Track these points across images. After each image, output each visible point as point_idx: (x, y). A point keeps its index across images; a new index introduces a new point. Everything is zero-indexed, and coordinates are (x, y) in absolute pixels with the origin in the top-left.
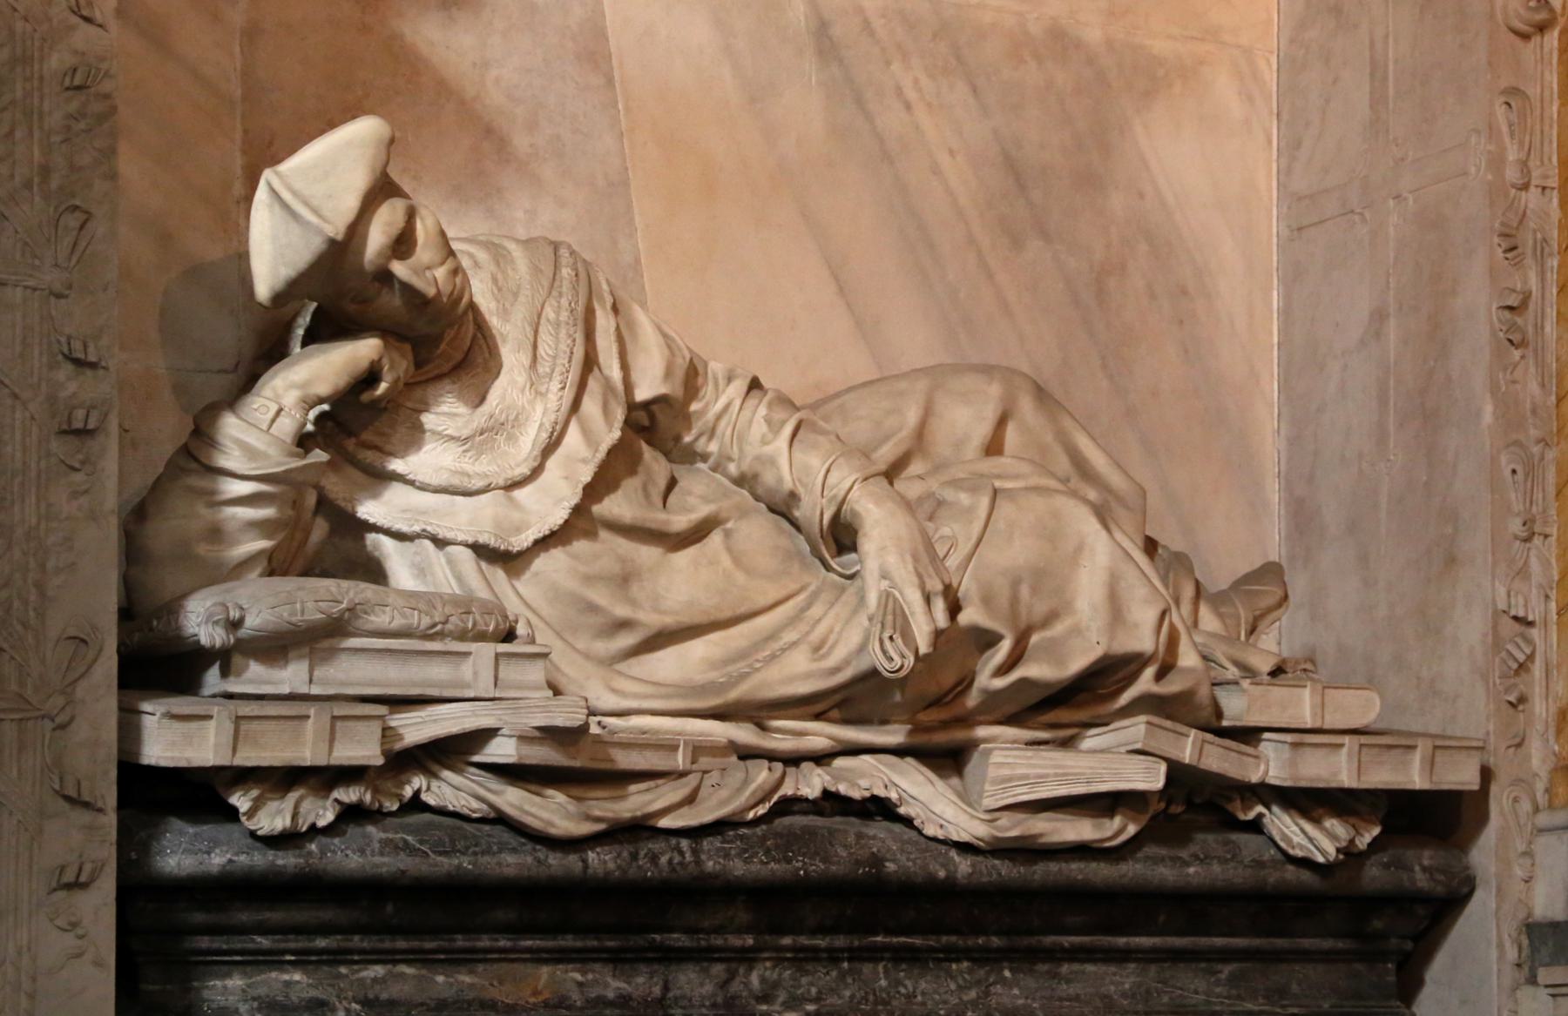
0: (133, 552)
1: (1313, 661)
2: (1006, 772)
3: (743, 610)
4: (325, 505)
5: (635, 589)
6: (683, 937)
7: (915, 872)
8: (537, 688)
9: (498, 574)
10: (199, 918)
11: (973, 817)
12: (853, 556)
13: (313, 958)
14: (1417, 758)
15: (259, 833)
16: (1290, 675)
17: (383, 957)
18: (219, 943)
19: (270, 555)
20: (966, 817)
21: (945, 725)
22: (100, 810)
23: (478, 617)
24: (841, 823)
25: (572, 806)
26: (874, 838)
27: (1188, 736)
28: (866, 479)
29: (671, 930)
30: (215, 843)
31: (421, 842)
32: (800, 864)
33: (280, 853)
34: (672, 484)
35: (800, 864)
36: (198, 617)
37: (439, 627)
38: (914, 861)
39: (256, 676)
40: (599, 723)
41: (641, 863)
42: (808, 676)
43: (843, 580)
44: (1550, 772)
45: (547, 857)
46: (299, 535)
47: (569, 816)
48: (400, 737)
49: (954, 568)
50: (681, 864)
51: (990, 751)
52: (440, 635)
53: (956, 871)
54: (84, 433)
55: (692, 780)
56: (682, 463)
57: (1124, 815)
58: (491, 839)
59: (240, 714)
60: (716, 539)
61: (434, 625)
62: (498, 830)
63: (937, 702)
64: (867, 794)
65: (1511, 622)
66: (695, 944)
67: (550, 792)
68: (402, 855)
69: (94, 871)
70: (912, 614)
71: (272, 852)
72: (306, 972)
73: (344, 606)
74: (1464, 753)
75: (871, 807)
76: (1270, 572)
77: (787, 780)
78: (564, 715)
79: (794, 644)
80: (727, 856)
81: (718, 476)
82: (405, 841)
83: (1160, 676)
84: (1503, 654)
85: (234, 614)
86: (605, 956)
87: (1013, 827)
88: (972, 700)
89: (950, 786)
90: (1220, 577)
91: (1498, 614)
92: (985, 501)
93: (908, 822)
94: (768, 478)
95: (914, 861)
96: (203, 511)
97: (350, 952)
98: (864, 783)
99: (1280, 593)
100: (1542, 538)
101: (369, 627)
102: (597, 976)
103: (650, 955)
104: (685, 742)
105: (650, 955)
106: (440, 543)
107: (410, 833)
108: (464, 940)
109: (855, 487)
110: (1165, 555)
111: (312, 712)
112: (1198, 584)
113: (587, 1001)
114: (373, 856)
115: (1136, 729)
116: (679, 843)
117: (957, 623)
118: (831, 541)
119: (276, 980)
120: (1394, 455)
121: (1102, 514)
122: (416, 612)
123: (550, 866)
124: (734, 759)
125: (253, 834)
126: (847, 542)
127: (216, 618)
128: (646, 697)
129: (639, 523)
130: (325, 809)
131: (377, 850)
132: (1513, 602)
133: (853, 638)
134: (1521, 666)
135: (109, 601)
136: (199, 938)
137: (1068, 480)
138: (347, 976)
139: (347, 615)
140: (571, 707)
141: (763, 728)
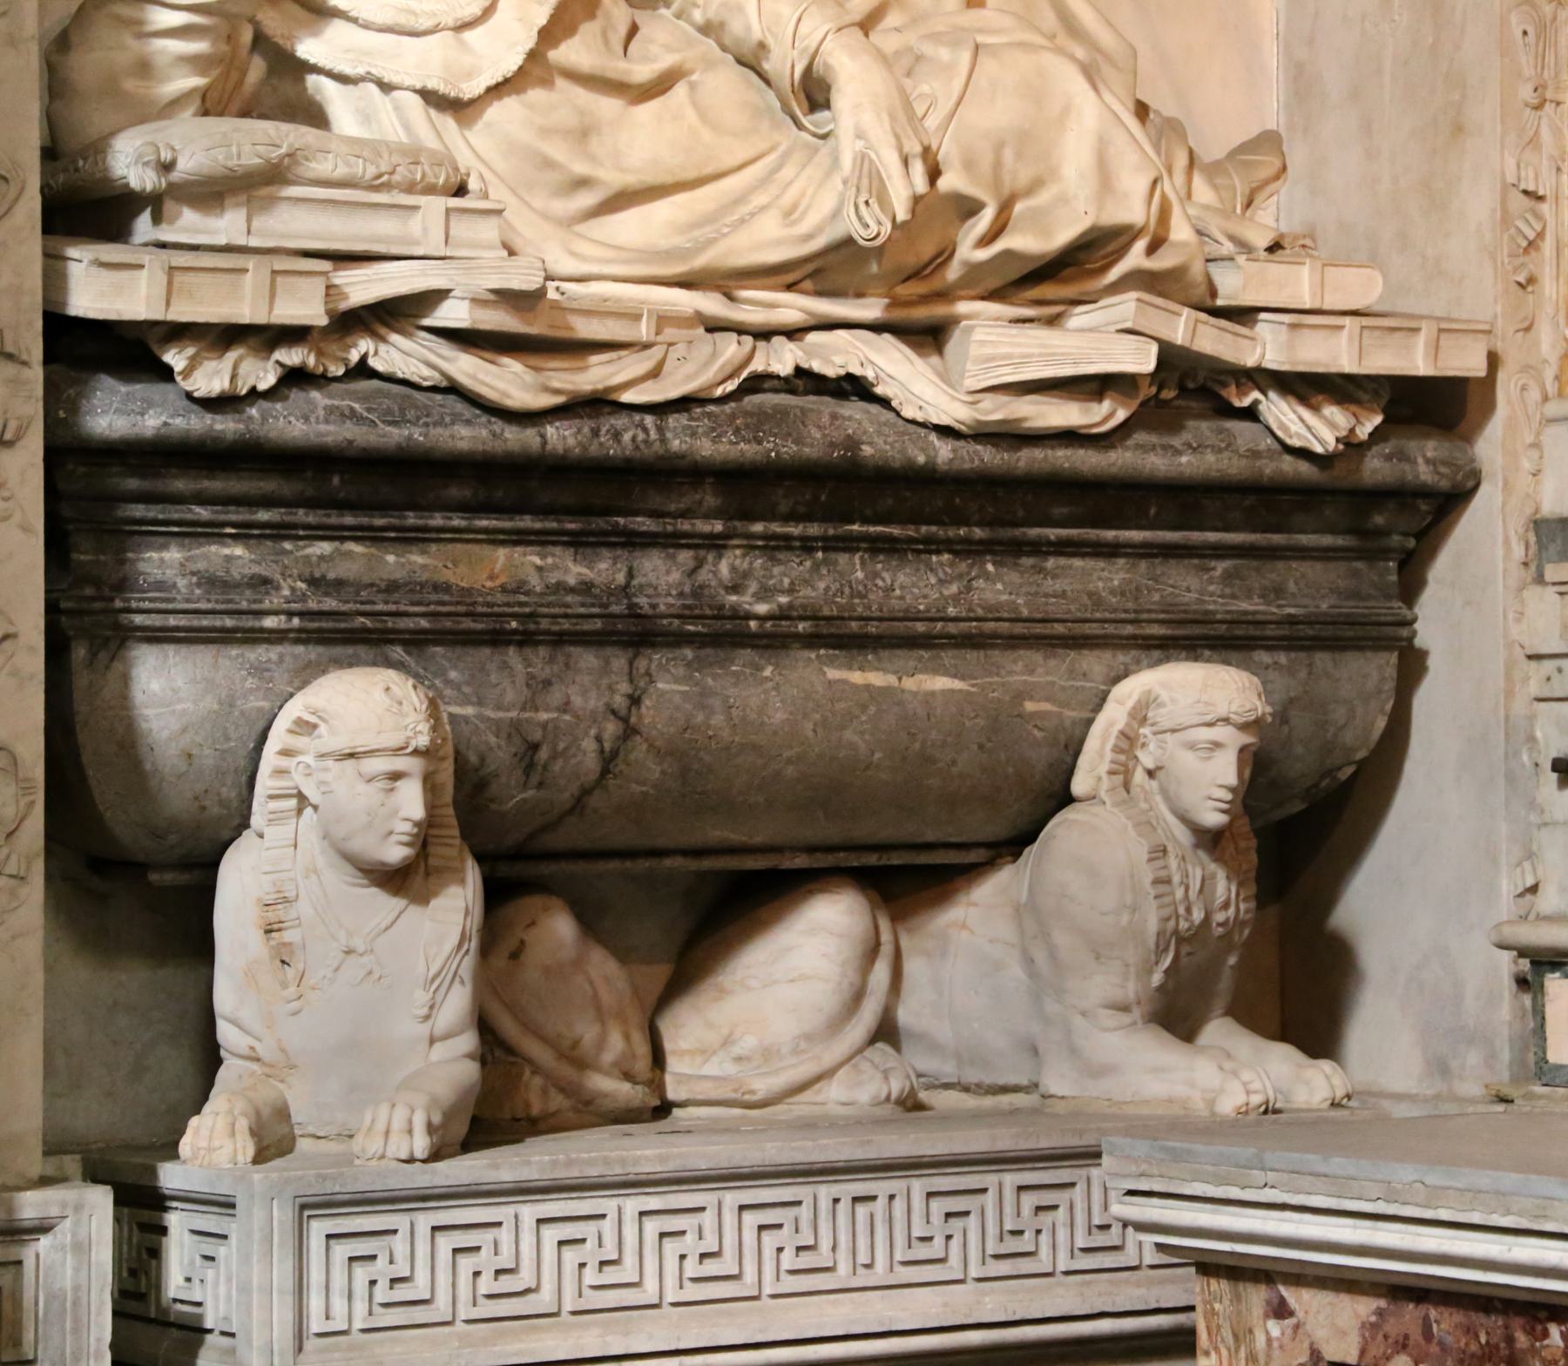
0: (56, 86)
1: (1314, 240)
2: (989, 351)
3: (709, 170)
4: (260, 41)
5: (594, 144)
6: (648, 521)
7: (893, 457)
8: (490, 247)
9: (448, 123)
10: (133, 484)
11: (954, 398)
12: (826, 114)
13: (256, 532)
14: (1421, 342)
15: (196, 394)
16: (1288, 251)
17: (328, 533)
18: (154, 512)
19: (204, 94)
20: (948, 398)
21: (926, 299)
22: (25, 363)
23: (427, 168)
24: (814, 403)
25: (529, 376)
26: (850, 418)
27: (1180, 315)
28: (839, 30)
29: (636, 513)
30: (150, 404)
31: (369, 410)
32: (771, 446)
33: (218, 417)
34: (633, 30)
35: (772, 445)
36: (127, 157)
37: (385, 178)
38: (891, 445)
39: (189, 224)
40: (558, 289)
41: (602, 439)
42: (779, 242)
43: (815, 140)
44: (1561, 358)
45: (503, 430)
46: (235, 75)
47: (525, 387)
48: (345, 297)
49: (933, 128)
50: (646, 442)
51: (971, 329)
52: (387, 187)
53: (936, 456)
55: (656, 353)
56: (644, 8)
57: (1113, 399)
58: (443, 410)
59: (173, 264)
60: (680, 91)
61: (380, 176)
62: (451, 399)
63: (916, 275)
64: (842, 372)
65: (1522, 196)
66: (660, 529)
67: (506, 360)
68: (348, 424)
69: (19, 428)
70: (889, 177)
71: (210, 415)
72: (248, 547)
73: (283, 151)
74: (1471, 336)
75: (847, 386)
76: (1269, 141)
77: (758, 354)
78: (522, 279)
79: (763, 209)
80: (694, 434)
81: (681, 23)
82: (352, 409)
83: (1152, 249)
84: (1513, 231)
85: (166, 155)
86: (565, 539)
87: (997, 410)
88: (953, 273)
89: (931, 366)
90: (1214, 148)
91: (1506, 188)
92: (965, 57)
93: (885, 402)
94: (736, 27)
95: (891, 445)
96: (131, 42)
97: (295, 526)
98: (838, 360)
99: (1278, 164)
100: (1553, 105)
101: (310, 175)
102: (557, 560)
103: (613, 539)
104: (649, 311)
105: (613, 539)
106: (386, 87)
107: (358, 400)
108: (416, 517)
109: (828, 38)
110: (1158, 120)
111: (250, 266)
112: (1191, 152)
113: (547, 587)
114: (318, 422)
115: (1126, 306)
116: (643, 420)
117: (937, 190)
118: (802, 96)
119: (216, 554)
120: (1400, 15)
121: (1090, 74)
122: (361, 161)
123: (506, 440)
124: (701, 330)
125: (189, 396)
126: (820, 98)
127: (146, 159)
128: (608, 261)
129: (598, 72)
130: (266, 371)
131: (321, 418)
132: (1523, 174)
133: (826, 203)
134: (1530, 243)
135: (31, 138)
136: (134, 506)
137: (1054, 36)
138: (292, 552)
139: (286, 160)
140: (527, 268)
141: (731, 298)
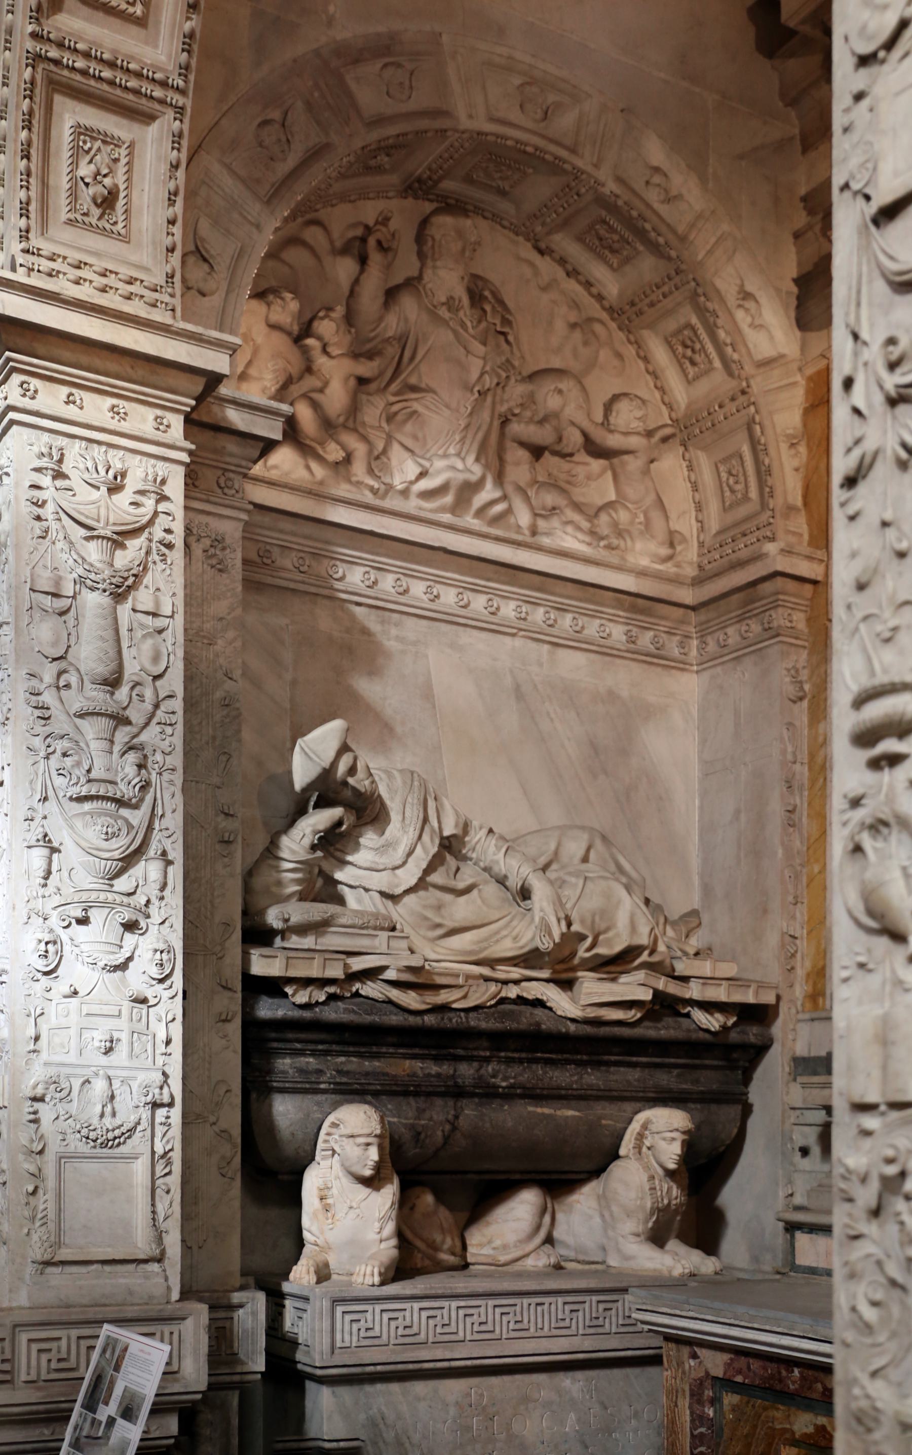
54: (228, 842)
